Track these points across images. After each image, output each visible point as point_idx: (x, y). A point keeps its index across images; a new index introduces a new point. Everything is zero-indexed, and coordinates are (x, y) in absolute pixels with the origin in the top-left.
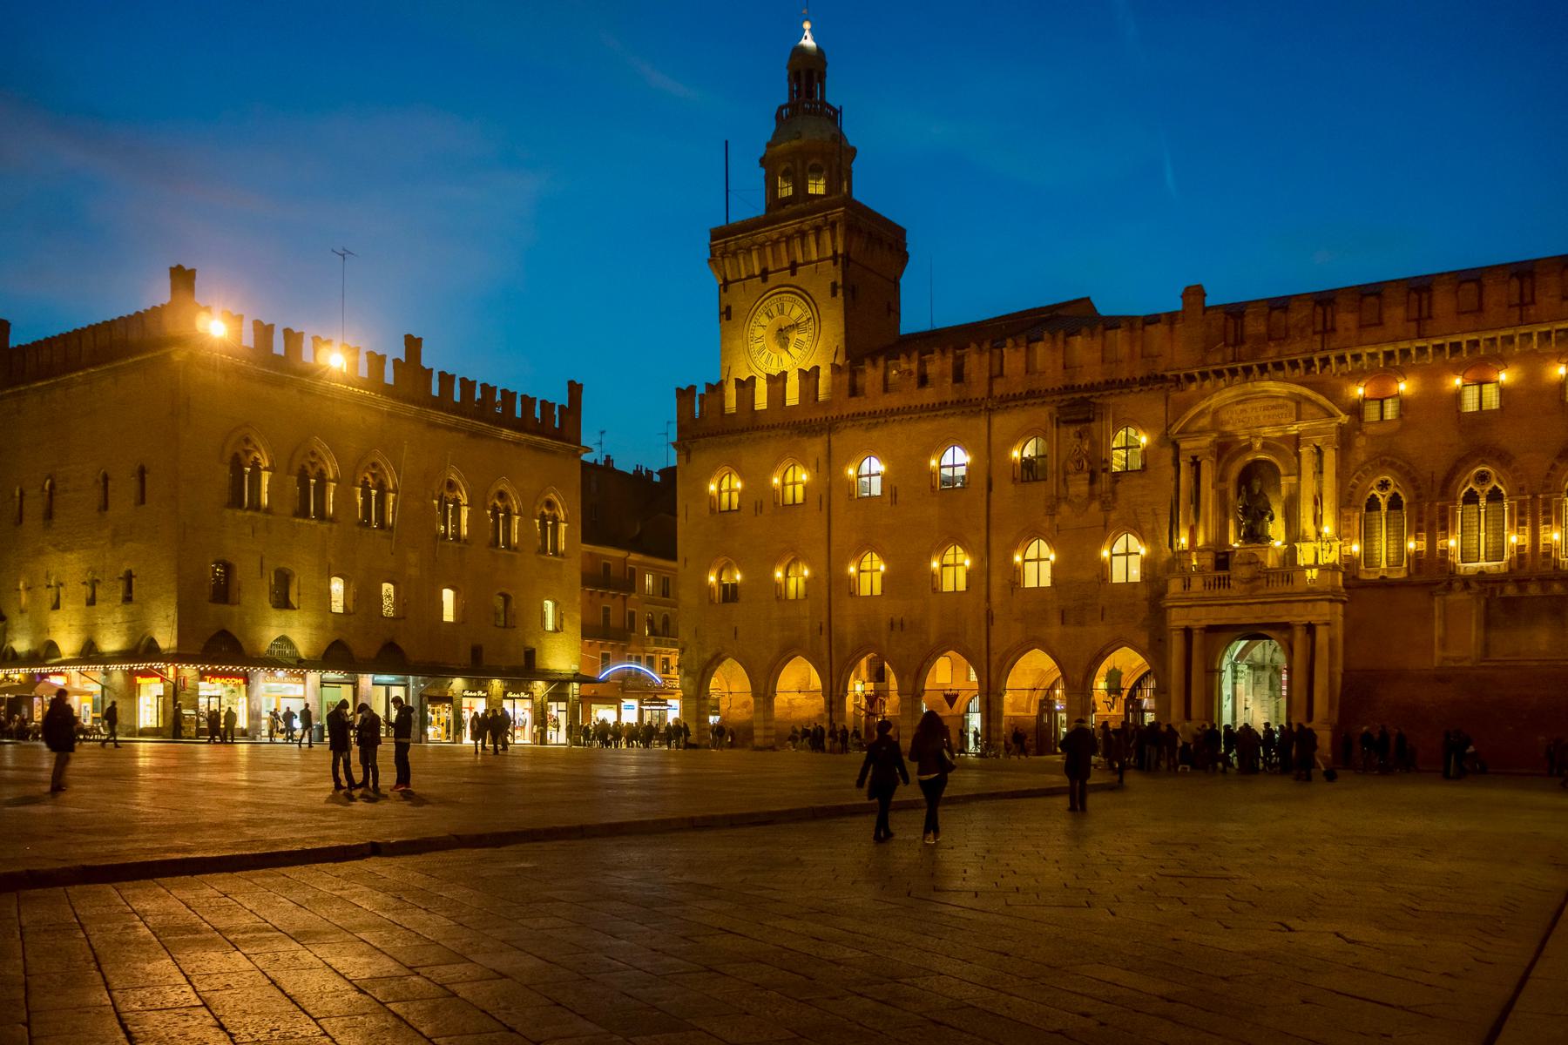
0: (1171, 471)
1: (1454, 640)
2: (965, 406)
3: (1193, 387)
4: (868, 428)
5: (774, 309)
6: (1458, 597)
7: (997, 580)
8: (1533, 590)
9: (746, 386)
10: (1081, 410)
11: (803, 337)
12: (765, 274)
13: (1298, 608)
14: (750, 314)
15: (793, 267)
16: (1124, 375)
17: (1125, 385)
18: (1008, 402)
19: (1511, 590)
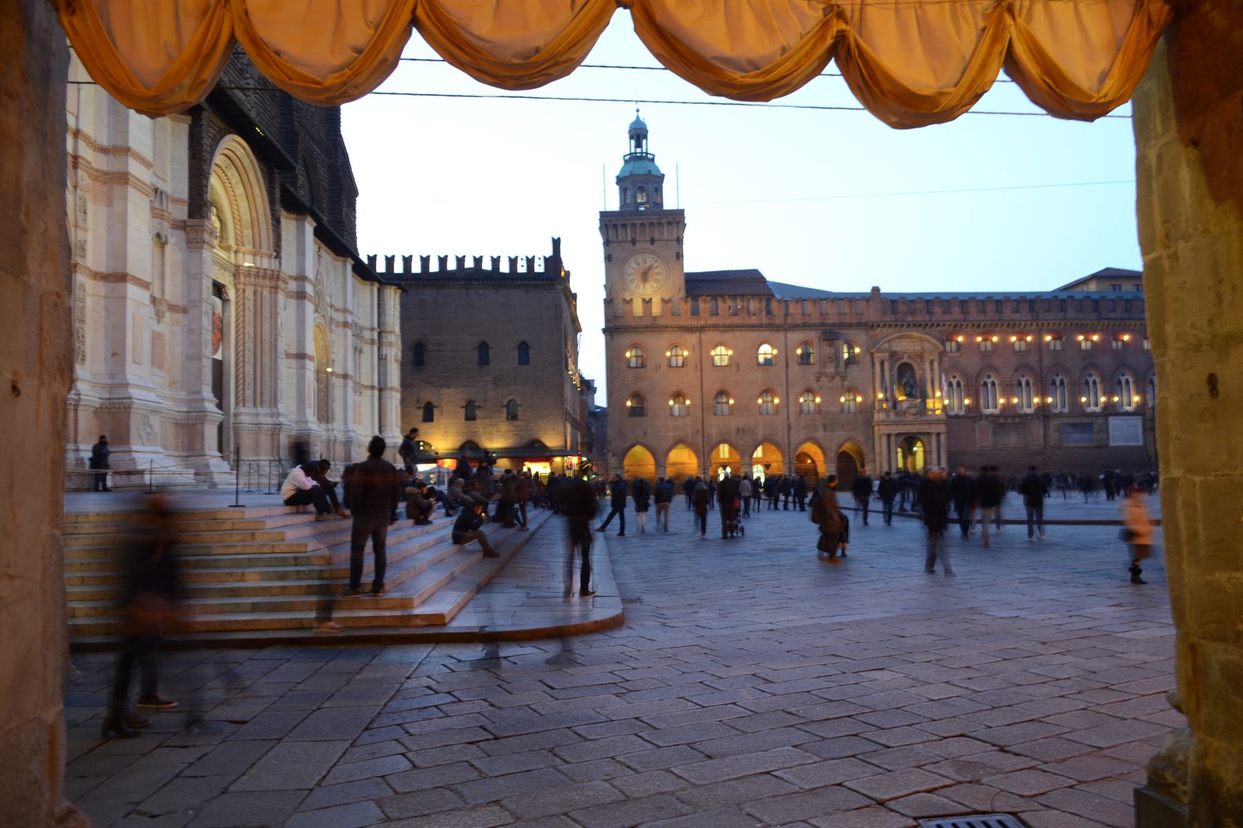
0: (870, 365)
1: (983, 439)
2: (773, 327)
3: (878, 330)
4: (723, 331)
5: (640, 261)
6: (984, 422)
7: (792, 409)
8: (1009, 421)
9: (647, 302)
10: (831, 334)
11: (659, 277)
12: (634, 242)
13: (934, 426)
14: (625, 261)
15: (652, 241)
16: (848, 321)
17: (849, 326)
18: (794, 327)
19: (1002, 420)
